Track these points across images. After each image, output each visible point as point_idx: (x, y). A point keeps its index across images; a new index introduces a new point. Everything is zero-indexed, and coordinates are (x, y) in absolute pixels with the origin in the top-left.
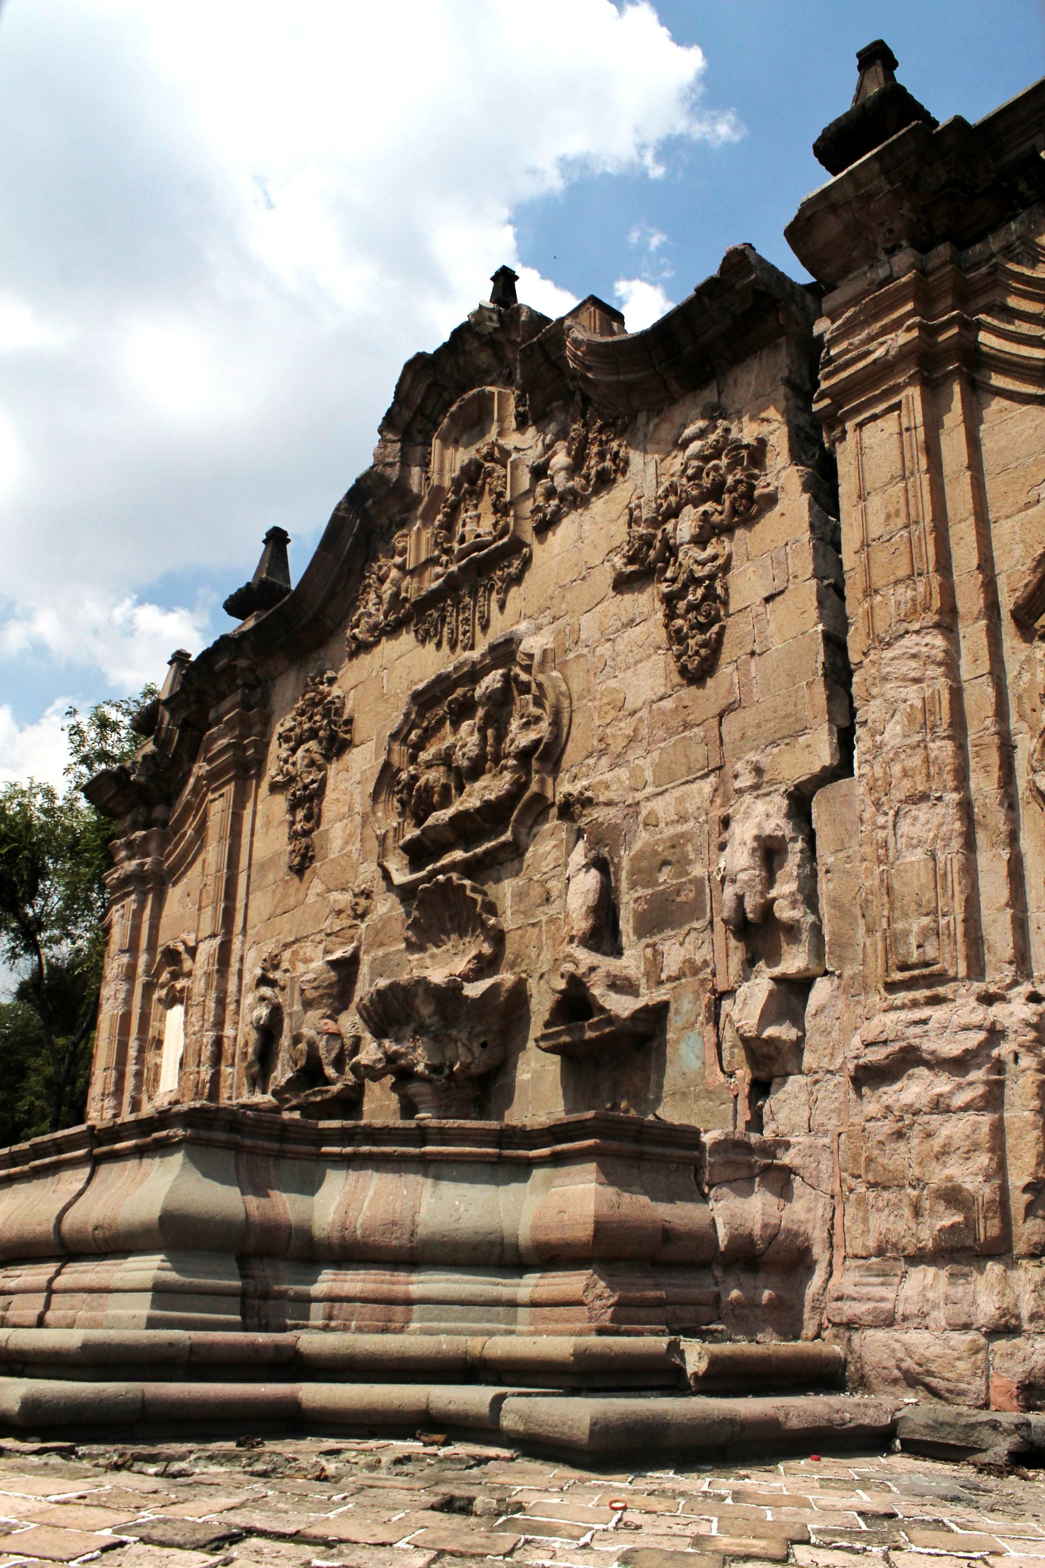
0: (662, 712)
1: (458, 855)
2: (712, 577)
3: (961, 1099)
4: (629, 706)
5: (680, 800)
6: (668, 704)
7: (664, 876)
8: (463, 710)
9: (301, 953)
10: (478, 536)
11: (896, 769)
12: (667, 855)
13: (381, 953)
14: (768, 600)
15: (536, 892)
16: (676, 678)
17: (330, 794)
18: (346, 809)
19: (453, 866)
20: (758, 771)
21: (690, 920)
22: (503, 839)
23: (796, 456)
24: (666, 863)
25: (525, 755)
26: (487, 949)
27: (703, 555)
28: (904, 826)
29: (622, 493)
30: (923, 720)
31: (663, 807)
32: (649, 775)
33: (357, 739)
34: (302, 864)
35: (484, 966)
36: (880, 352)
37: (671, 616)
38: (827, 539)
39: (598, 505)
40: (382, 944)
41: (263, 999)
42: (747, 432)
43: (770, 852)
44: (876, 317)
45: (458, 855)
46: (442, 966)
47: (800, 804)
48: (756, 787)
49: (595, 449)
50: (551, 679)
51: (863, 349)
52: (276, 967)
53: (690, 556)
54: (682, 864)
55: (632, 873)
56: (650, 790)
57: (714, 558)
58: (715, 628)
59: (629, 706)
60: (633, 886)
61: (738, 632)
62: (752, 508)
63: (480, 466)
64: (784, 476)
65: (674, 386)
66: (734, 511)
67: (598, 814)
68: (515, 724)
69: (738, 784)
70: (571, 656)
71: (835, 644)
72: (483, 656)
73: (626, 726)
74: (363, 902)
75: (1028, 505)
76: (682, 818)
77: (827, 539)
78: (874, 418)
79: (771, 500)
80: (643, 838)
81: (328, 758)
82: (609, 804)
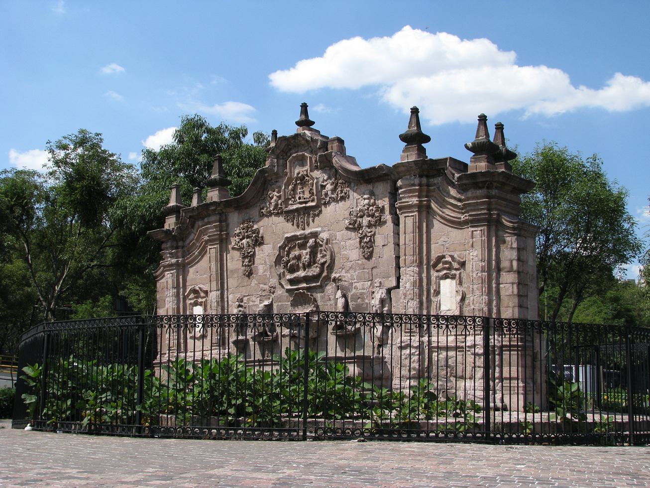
0: (358, 264)
1: (304, 285)
3: (416, 353)
5: (363, 285)
6: (360, 262)
8: (303, 246)
10: (304, 199)
11: (408, 293)
12: (360, 296)
13: (280, 304)
15: (327, 297)
16: (362, 257)
17: (257, 257)
19: (303, 288)
20: (380, 283)
22: (318, 284)
23: (391, 213)
25: (323, 264)
26: (315, 309)
27: (369, 230)
28: (409, 304)
29: (347, 203)
30: (414, 283)
31: (359, 285)
32: (355, 277)
33: (265, 242)
34: (249, 274)
36: (411, 203)
37: (360, 242)
38: (397, 234)
39: (341, 204)
40: (280, 302)
42: (380, 203)
43: (382, 301)
44: (410, 193)
45: (304, 285)
46: (301, 311)
47: (389, 291)
48: (380, 286)
49: (340, 189)
50: (329, 247)
52: (242, 302)
53: (366, 230)
54: (363, 299)
55: (351, 298)
56: (355, 281)
57: (371, 232)
58: (371, 249)
60: (351, 301)
61: (376, 250)
62: (380, 223)
63: (304, 178)
64: (387, 217)
67: (343, 283)
68: (319, 256)
69: (376, 285)
70: (334, 242)
71: (398, 258)
73: (349, 264)
74: (272, 289)
75: (436, 243)
77: (397, 234)
79: (385, 222)
81: (255, 245)
82: (345, 281)
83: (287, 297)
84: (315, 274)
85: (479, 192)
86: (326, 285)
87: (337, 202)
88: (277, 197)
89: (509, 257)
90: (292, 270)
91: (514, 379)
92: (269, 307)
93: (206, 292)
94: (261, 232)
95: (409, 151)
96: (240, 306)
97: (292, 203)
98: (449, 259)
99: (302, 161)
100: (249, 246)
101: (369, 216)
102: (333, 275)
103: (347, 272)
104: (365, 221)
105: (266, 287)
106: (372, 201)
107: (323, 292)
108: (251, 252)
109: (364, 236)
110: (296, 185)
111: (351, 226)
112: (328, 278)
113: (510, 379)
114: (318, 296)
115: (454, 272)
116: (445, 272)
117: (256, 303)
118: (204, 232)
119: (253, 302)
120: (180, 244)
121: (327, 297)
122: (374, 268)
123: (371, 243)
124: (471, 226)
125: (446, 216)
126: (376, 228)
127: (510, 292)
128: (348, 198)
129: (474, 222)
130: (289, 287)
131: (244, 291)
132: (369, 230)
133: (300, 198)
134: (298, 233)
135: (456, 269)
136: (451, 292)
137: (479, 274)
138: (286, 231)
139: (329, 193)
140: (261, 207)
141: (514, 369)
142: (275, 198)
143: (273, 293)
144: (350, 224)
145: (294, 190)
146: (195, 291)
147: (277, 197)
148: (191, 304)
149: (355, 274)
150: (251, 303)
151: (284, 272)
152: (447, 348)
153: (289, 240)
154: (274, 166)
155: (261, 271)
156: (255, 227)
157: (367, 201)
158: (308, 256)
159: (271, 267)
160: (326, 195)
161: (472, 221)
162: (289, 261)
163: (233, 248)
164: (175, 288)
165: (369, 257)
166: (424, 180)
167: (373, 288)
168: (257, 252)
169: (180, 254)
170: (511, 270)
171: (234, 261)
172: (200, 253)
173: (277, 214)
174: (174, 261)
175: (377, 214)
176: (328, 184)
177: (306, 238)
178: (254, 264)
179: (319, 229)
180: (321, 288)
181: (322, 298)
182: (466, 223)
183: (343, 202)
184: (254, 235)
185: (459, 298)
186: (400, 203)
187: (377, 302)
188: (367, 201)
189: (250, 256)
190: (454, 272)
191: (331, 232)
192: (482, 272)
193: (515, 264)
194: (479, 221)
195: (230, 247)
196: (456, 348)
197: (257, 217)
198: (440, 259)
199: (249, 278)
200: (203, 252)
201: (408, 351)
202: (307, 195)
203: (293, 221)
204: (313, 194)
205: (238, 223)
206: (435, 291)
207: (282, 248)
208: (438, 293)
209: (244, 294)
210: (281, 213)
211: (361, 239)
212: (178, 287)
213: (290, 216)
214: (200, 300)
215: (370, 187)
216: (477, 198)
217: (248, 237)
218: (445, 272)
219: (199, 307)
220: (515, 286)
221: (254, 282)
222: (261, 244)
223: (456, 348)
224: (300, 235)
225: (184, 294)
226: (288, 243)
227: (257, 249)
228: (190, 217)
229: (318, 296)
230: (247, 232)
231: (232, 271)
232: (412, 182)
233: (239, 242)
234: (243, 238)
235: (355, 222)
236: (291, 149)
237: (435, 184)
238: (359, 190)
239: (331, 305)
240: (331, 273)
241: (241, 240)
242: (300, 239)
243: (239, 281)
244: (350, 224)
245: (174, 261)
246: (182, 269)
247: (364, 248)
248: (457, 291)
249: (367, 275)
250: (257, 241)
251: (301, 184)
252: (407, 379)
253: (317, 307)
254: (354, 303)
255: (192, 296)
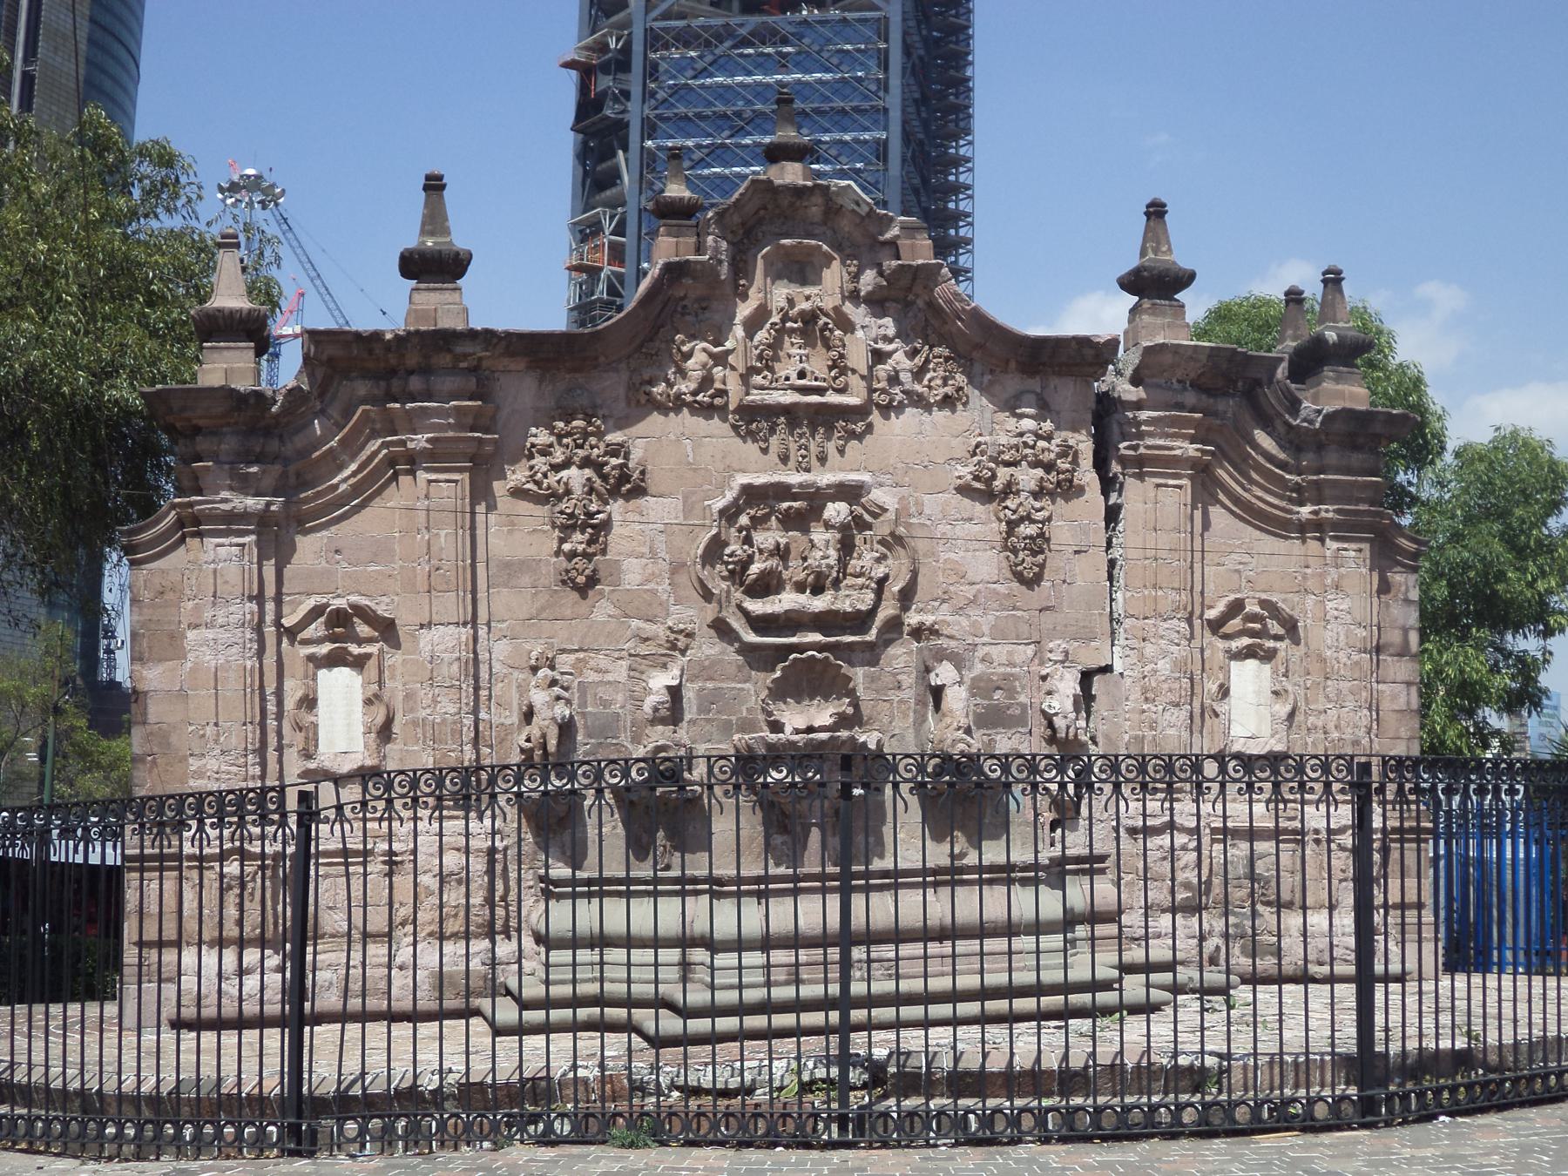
2: (1043, 522)
4: (970, 576)
5: (1010, 653)
7: (998, 695)
9: (592, 663)
11: (1165, 686)
13: (710, 685)
14: (1076, 552)
15: (888, 679)
17: (617, 529)
18: (646, 550)
20: (1066, 653)
21: (1018, 725)
24: (999, 688)
25: (882, 582)
26: (850, 710)
27: (1038, 505)
28: (1167, 715)
29: (962, 417)
30: (1180, 666)
31: (999, 652)
32: (985, 629)
33: (652, 490)
35: (843, 721)
39: (940, 415)
40: (711, 679)
41: (558, 698)
45: (816, 637)
47: (1086, 677)
48: (1062, 662)
51: (1168, 443)
54: (1011, 693)
56: (985, 639)
59: (970, 576)
61: (1054, 562)
62: (1068, 490)
64: (1087, 476)
65: (1013, 365)
66: (1059, 483)
72: (829, 486)
73: (970, 592)
76: (1012, 664)
78: (1166, 486)
79: (1081, 491)
80: (979, 668)
81: (614, 493)
82: (951, 637)
83: (740, 669)
84: (863, 608)
85: (1356, 459)
86: (888, 643)
87: (928, 408)
88: (711, 355)
89: (1401, 622)
90: (766, 586)
91: (1411, 906)
92: (675, 692)
93: (387, 630)
94: (636, 454)
95: (1164, 314)
96: (553, 683)
97: (767, 383)
98: (1257, 609)
99: (801, 270)
100: (591, 490)
101: (1036, 464)
102: (912, 619)
103: (959, 611)
104: (1028, 477)
105: (659, 630)
106: (1048, 426)
107: (874, 662)
108: (599, 512)
109: (1022, 520)
110: (781, 332)
111: (977, 485)
112: (894, 627)
113: (1403, 906)
114: (859, 675)
115: (1270, 644)
116: (1246, 641)
117: (609, 677)
118: (413, 423)
119: (598, 671)
120: (274, 445)
121: (888, 679)
122: (1047, 609)
123: (1039, 544)
124: (1332, 538)
125: (1254, 500)
126: (1053, 502)
127: (1401, 703)
128: (965, 404)
129: (1345, 529)
130: (751, 637)
131: (562, 634)
132: (1038, 505)
133: (802, 375)
134: (795, 479)
135: (1277, 638)
136: (1258, 693)
137: (1356, 657)
138: (735, 466)
139: (905, 377)
140: (646, 377)
141: (1411, 883)
142: (699, 358)
143: (683, 652)
144: (977, 478)
145: (776, 345)
146: (340, 621)
147: (711, 355)
148: (311, 658)
149: (986, 622)
150: (592, 677)
151: (728, 592)
152: (1252, 834)
153: (751, 494)
154: (720, 262)
155: (633, 573)
156: (615, 437)
157: (1028, 424)
158: (833, 553)
159: (676, 568)
160: (894, 379)
161: (1335, 526)
162: (750, 560)
163: (518, 493)
164: (251, 598)
165: (1032, 582)
166: (1206, 401)
167: (1042, 663)
168: (616, 517)
169: (268, 482)
170: (1403, 652)
171: (520, 534)
172: (356, 490)
173: (707, 411)
174: (253, 503)
175: (1063, 464)
176: (896, 351)
177: (816, 499)
178: (604, 552)
179: (866, 477)
180: (871, 655)
181: (873, 679)
182: (1318, 528)
183: (947, 412)
184: (614, 461)
185: (1283, 709)
186: (1148, 447)
187: (1069, 705)
188: (1028, 424)
189: (593, 527)
190: (1270, 644)
191: (904, 491)
192: (1360, 651)
193: (1414, 638)
194: (1353, 527)
195: (499, 487)
196: (1276, 834)
197: (622, 404)
198: (1236, 607)
199: (584, 596)
200: (367, 490)
201: (1165, 840)
202: (818, 364)
203: (766, 440)
204: (843, 371)
205: (537, 410)
206: (1221, 686)
207: (729, 514)
208: (1224, 692)
209: (557, 645)
210: (722, 411)
211: (1012, 525)
212: (259, 598)
213: (754, 420)
214: (354, 649)
215: (1035, 384)
216: (1348, 472)
217: (586, 463)
218: (1246, 641)
219: (346, 670)
220: (1414, 690)
221: (602, 610)
222: (639, 491)
223: (1276, 834)
224: (801, 485)
225: (278, 623)
226: (748, 504)
227: (616, 508)
228: (330, 360)
229: (859, 675)
230: (581, 447)
231: (507, 565)
232: (1180, 398)
233: (545, 476)
234: (566, 464)
235: (994, 477)
236: (760, 222)
237: (1215, 414)
238: (997, 388)
239: (901, 701)
240: (905, 608)
241: (557, 468)
242: (795, 498)
243: (543, 599)
244: (977, 478)
245: (253, 503)
246: (275, 539)
247: (1015, 551)
248: (1276, 693)
249: (1026, 627)
250: (624, 477)
251: (803, 333)
252: (1164, 911)
253: (855, 704)
254: (979, 701)
255: (316, 629)
